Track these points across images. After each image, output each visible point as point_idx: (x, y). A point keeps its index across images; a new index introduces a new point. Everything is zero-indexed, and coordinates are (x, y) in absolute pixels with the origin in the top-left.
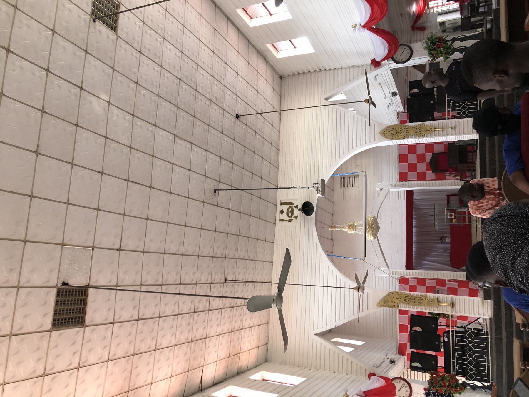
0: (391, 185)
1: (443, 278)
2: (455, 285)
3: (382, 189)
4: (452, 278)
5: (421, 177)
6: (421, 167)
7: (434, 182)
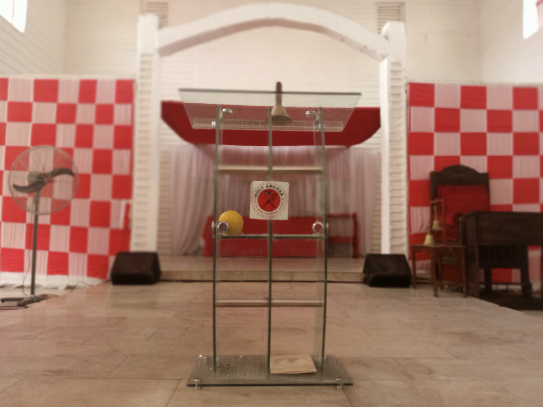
0: (398, 64)
1: (136, 192)
2: (117, 223)
3: (386, 37)
4: (135, 215)
5: (418, 144)
6: (447, 145)
7: (404, 176)
